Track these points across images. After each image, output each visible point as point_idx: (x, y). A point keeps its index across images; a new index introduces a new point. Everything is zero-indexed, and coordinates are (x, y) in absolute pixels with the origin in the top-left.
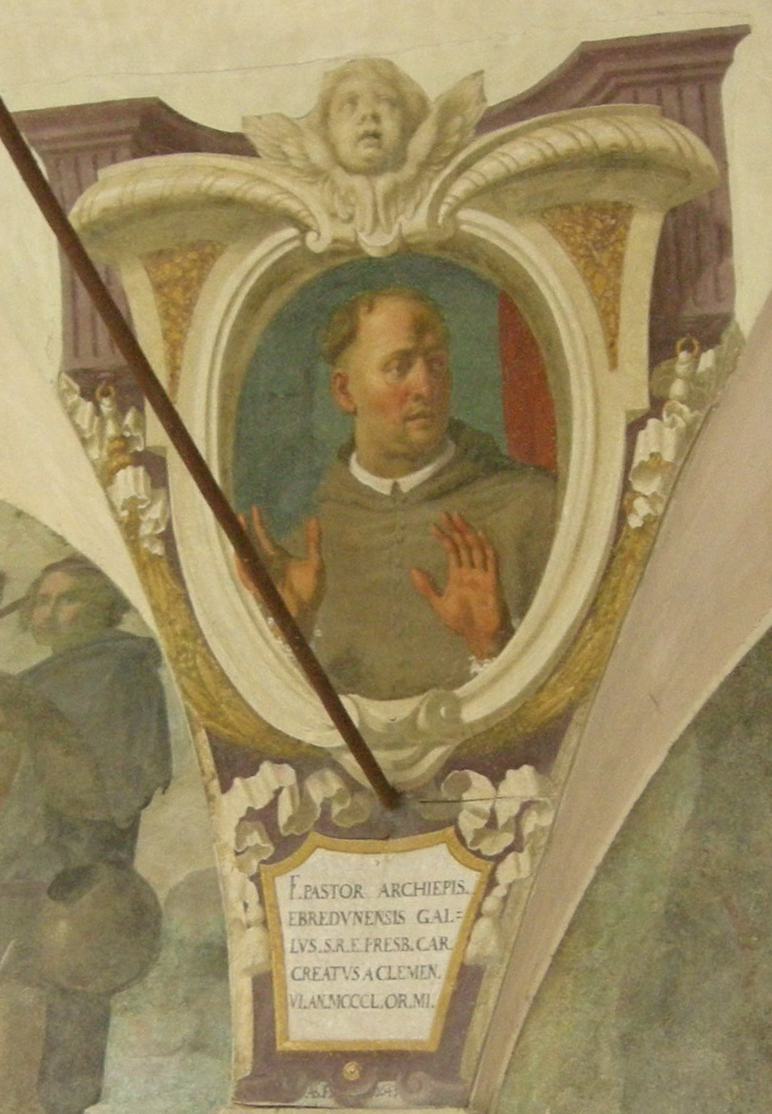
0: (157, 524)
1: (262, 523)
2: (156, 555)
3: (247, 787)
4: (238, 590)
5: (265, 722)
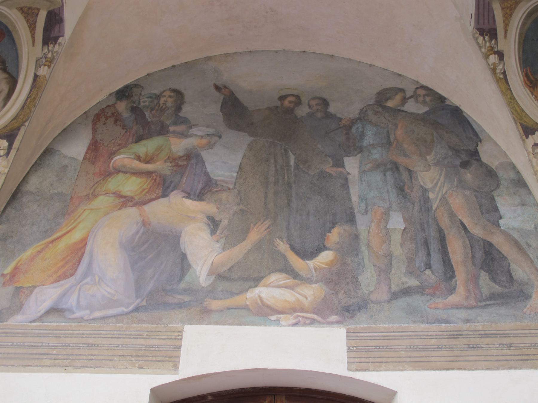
0: (501, 70)
1: (530, 72)
2: (501, 78)
3: (533, 138)
4: (524, 88)
5: (535, 122)
